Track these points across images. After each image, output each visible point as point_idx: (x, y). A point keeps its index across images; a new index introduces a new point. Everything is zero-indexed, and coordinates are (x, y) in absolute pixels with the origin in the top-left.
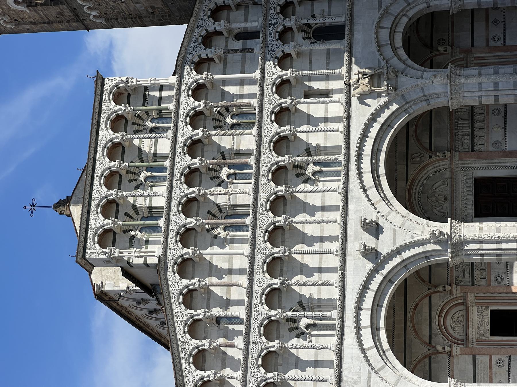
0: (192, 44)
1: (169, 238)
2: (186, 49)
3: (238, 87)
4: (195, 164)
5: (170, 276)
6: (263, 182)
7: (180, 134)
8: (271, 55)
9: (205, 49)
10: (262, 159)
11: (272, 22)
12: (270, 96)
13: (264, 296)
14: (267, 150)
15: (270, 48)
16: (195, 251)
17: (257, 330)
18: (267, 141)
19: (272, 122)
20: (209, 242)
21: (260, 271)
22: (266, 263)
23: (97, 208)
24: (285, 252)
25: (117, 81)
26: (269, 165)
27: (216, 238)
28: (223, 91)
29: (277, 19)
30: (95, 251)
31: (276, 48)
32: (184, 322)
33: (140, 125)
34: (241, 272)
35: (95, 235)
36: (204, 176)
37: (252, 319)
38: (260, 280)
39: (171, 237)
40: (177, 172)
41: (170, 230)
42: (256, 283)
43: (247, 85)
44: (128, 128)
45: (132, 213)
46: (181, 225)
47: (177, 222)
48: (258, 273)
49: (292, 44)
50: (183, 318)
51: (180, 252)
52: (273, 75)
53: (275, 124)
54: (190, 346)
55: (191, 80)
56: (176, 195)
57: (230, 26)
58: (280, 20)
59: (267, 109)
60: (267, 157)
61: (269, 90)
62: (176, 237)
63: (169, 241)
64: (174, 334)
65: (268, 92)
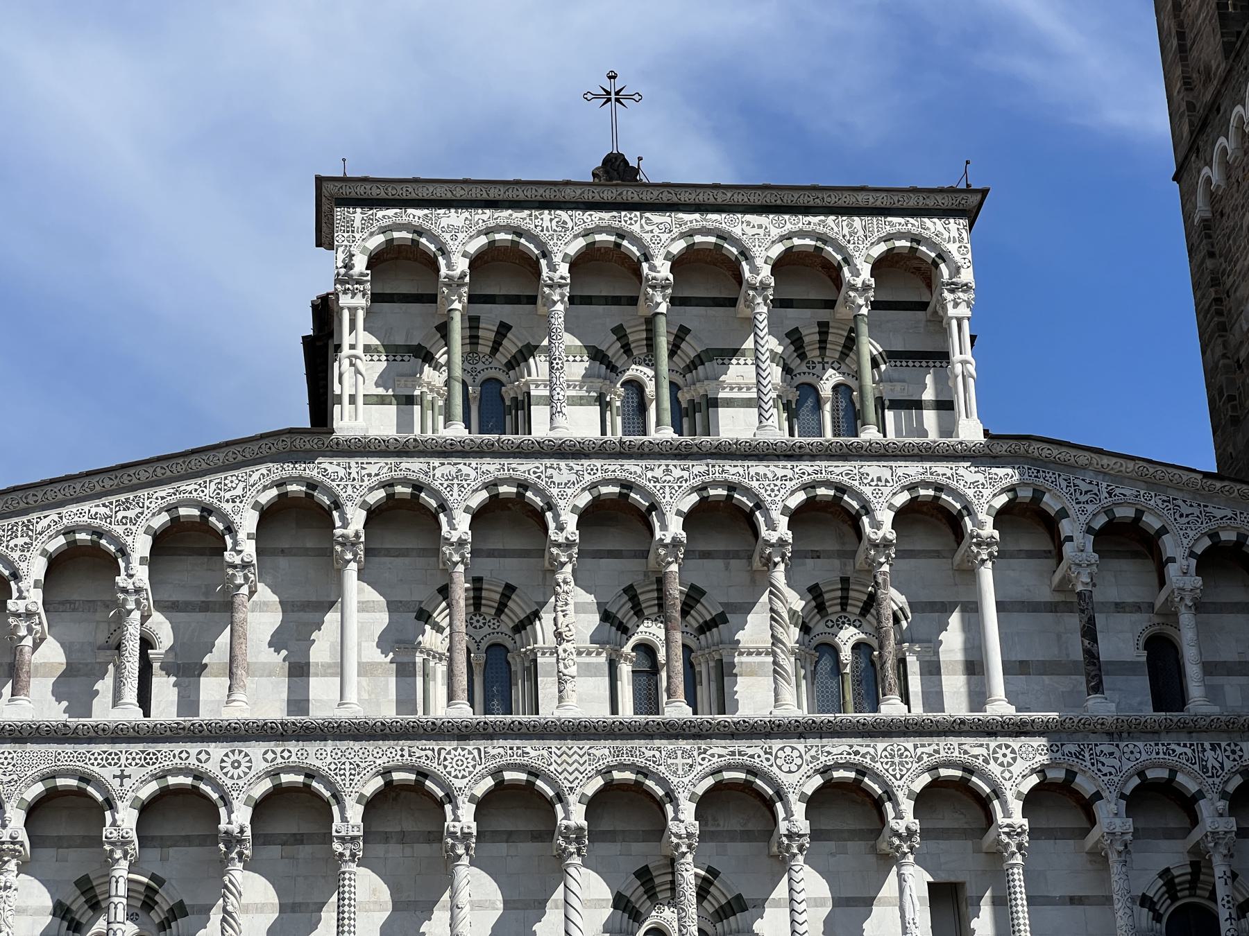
0: (1105, 485)
1: (398, 460)
2: (1084, 468)
3: (959, 656)
4: (664, 527)
5: (265, 472)
6: (598, 753)
7: (772, 468)
8: (1079, 755)
9: (1090, 530)
10: (682, 744)
11: (1209, 754)
12: (920, 759)
13: (189, 781)
14: (715, 760)
15: (1106, 748)
16: (353, 544)
17: (64, 764)
18: (752, 756)
19: (825, 771)
20: (402, 595)
21: (279, 760)
22: (308, 781)
23: (507, 229)
24: (343, 840)
25: (957, 257)
26: (662, 768)
27: (418, 618)
28: (945, 609)
29: (1222, 768)
30: (357, 236)
31: (1105, 770)
32: (105, 525)
33: (822, 348)
34: (298, 703)
35: (415, 232)
36: (634, 565)
37: (105, 747)
38: (243, 768)
39: (403, 466)
40: (633, 469)
41: (427, 460)
42: (233, 752)
43: (969, 683)
44: (807, 313)
45: (510, 346)
46: (445, 493)
47: (455, 481)
48: (270, 756)
49: (1124, 825)
50: (122, 522)
51: (350, 498)
52: (1002, 764)
53: (818, 781)
54: (19, 553)
55: (970, 493)
56: (550, 471)
57: (1183, 609)
58: (1217, 781)
59: (872, 751)
60: (690, 761)
61: (943, 753)
62: (404, 482)
63: (389, 460)
64: (60, 496)
65: (937, 752)
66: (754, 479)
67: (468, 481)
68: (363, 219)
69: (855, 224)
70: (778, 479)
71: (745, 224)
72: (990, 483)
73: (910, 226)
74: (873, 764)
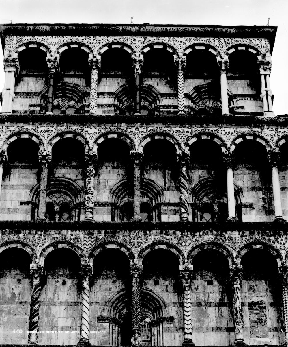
39: (25, 127)
55: (269, 139)
56: (87, 129)
66: (175, 132)
67: (52, 133)
68: (17, 40)
69: (222, 41)
70: (185, 132)
71: (175, 41)
72: (278, 135)
73: (245, 42)
74: (223, 243)
